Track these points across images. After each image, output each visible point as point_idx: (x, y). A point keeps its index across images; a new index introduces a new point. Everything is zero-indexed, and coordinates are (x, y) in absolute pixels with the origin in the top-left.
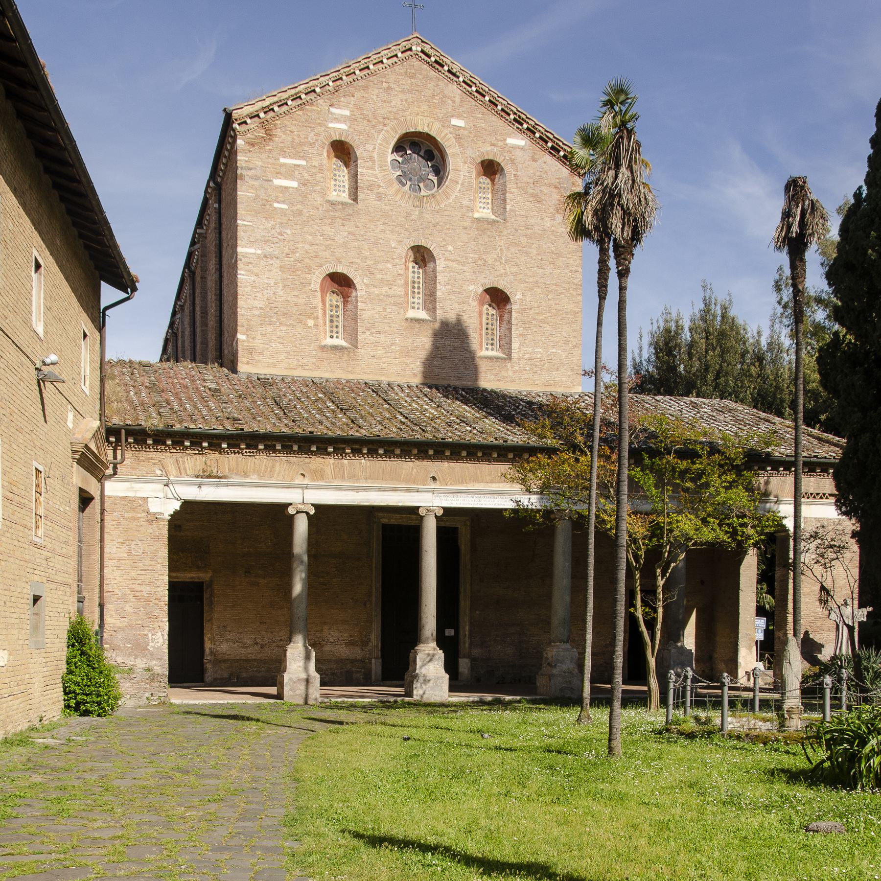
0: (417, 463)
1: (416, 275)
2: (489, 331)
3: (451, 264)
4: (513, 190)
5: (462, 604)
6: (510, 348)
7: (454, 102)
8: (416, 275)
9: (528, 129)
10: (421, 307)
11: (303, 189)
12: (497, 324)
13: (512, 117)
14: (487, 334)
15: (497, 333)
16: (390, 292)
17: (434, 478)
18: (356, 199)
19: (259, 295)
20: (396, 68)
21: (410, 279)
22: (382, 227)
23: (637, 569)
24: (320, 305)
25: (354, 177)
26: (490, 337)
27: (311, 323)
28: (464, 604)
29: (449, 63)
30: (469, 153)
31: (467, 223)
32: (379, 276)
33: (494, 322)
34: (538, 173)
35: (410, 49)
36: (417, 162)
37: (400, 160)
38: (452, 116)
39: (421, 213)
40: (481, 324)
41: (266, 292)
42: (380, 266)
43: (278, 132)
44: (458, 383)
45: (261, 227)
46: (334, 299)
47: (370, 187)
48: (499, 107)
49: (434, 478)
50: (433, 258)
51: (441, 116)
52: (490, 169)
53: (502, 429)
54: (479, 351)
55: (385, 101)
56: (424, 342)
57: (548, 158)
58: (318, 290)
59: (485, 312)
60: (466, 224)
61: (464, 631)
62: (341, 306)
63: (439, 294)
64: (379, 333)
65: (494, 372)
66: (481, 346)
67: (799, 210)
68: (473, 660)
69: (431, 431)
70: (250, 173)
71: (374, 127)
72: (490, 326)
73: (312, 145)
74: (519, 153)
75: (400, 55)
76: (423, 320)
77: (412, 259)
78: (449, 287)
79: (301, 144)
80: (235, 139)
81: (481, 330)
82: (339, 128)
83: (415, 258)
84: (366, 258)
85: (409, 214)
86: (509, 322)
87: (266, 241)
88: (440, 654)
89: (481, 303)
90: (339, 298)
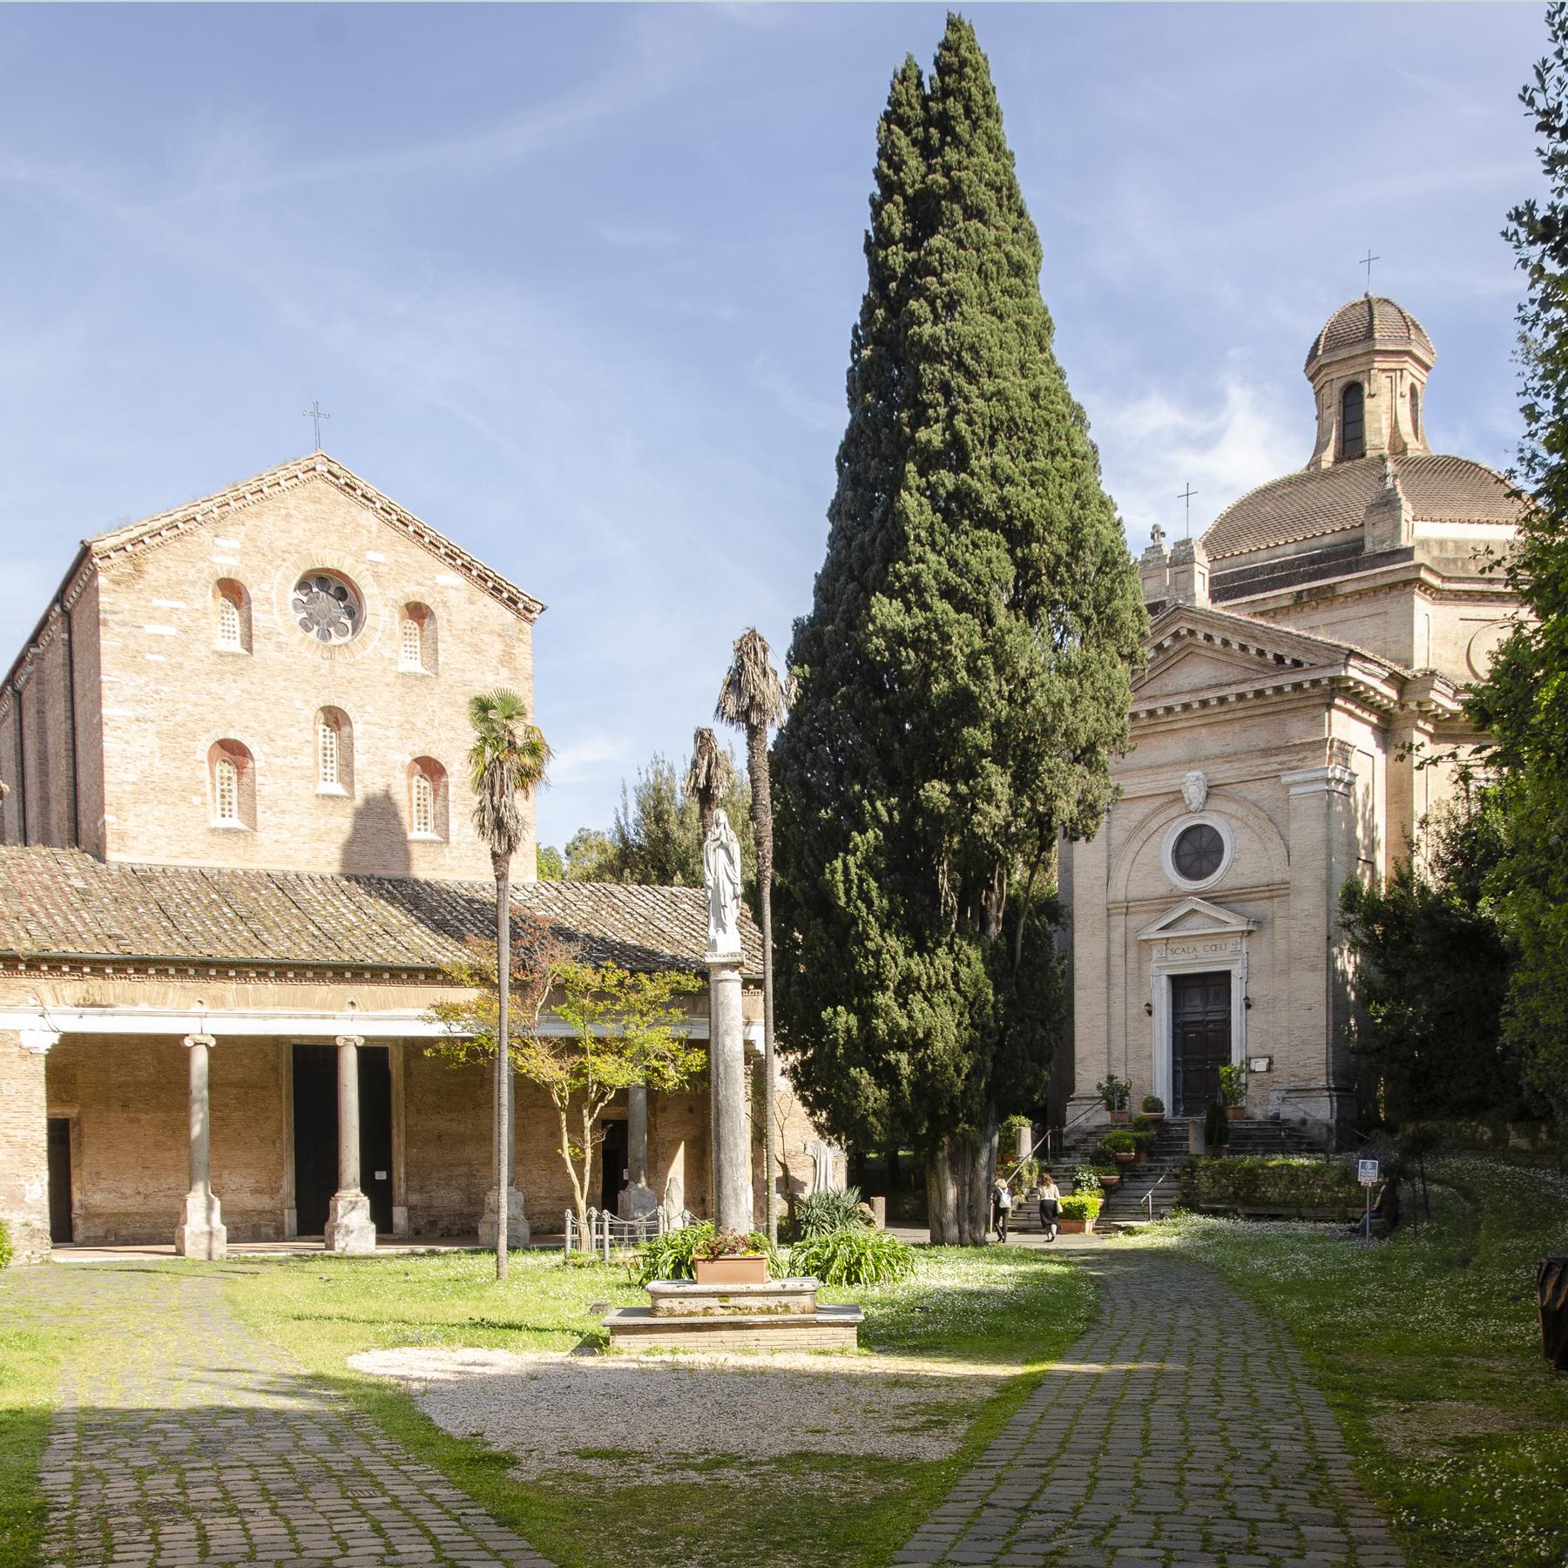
0: (332, 986)
1: (328, 740)
2: (422, 808)
3: (370, 728)
4: (446, 639)
5: (395, 1140)
6: (448, 830)
7: (370, 532)
8: (328, 740)
9: (463, 565)
10: (335, 778)
11: (184, 637)
12: (430, 799)
13: (443, 550)
14: (418, 811)
15: (431, 810)
16: (296, 763)
17: (352, 1004)
18: (250, 649)
19: (131, 767)
20: (297, 490)
21: (321, 745)
22: (283, 684)
23: (562, 1110)
24: (208, 778)
25: (248, 622)
26: (422, 814)
27: (197, 800)
28: (398, 1140)
29: (362, 485)
30: (391, 593)
31: (390, 678)
32: (281, 743)
33: (427, 796)
34: (477, 619)
35: (314, 469)
36: (325, 601)
37: (305, 599)
38: (369, 549)
39: (332, 666)
40: (411, 800)
41: (138, 763)
42: (282, 732)
43: (149, 568)
44: (382, 873)
45: (132, 684)
46: (226, 770)
47: (267, 637)
48: (427, 539)
49: (352, 1004)
50: (348, 722)
51: (354, 549)
52: (418, 612)
53: (432, 943)
54: (408, 833)
55: (284, 531)
56: (342, 824)
57: (489, 600)
58: (206, 760)
59: (415, 784)
60: (388, 680)
61: (399, 1173)
62: (235, 778)
63: (357, 765)
64: (283, 812)
65: (428, 859)
66: (412, 827)
67: (706, 762)
68: (411, 1208)
69: (349, 949)
70: (114, 617)
71: (270, 562)
72: (422, 802)
73: (193, 583)
74: (452, 594)
75: (301, 476)
76: (337, 797)
77: (322, 720)
78: (368, 756)
79: (180, 583)
80: (94, 574)
81: (411, 807)
82: (228, 565)
83: (326, 719)
84: (265, 721)
85: (316, 668)
86: (446, 798)
87: (138, 701)
88: (365, 1201)
89: (411, 774)
90: (231, 768)
